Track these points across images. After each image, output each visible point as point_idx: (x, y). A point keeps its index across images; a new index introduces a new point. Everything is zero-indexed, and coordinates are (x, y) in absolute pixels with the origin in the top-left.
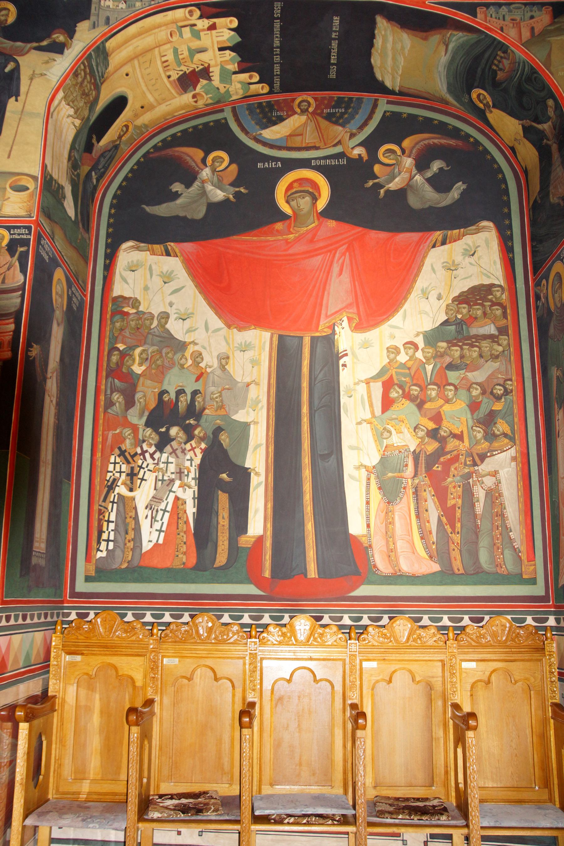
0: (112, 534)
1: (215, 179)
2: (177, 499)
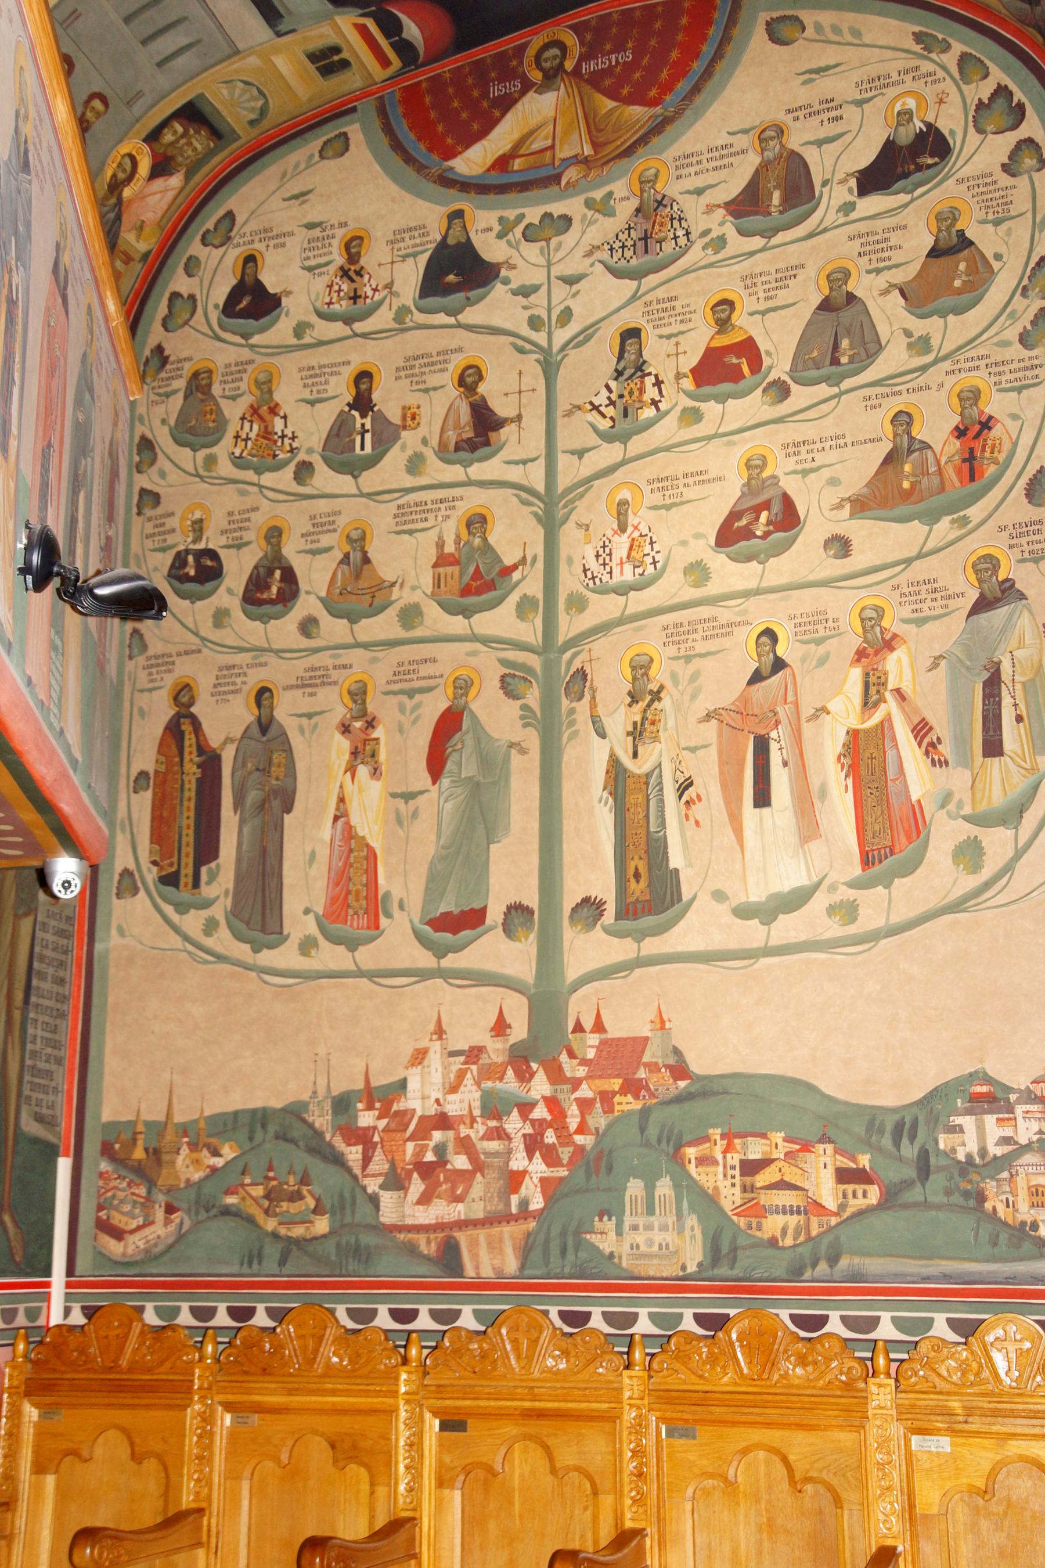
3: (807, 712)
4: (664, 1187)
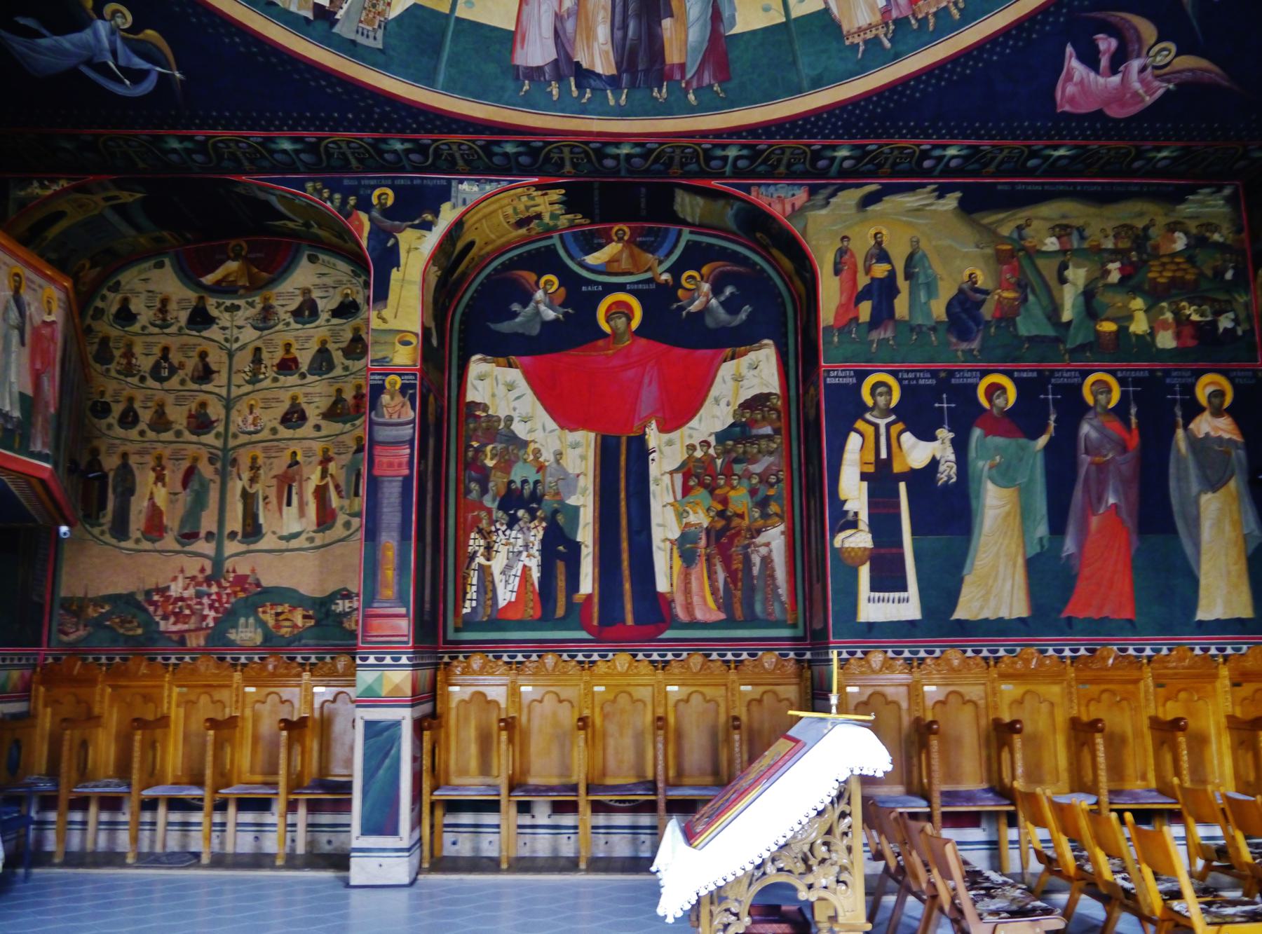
0: (475, 594)
1: (547, 300)
2: (525, 566)
3: (304, 478)
4: (251, 620)
